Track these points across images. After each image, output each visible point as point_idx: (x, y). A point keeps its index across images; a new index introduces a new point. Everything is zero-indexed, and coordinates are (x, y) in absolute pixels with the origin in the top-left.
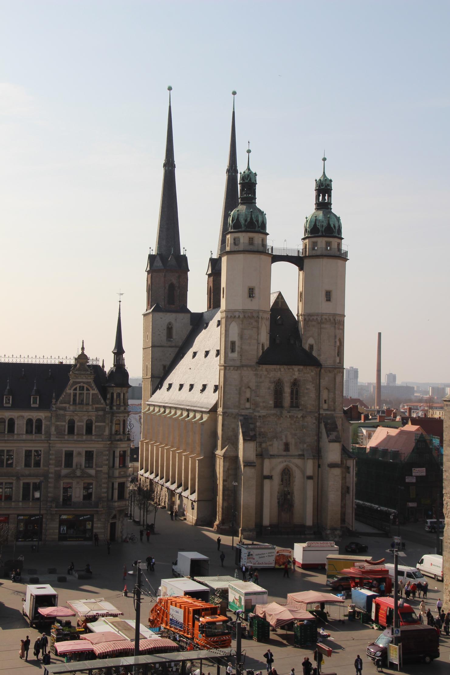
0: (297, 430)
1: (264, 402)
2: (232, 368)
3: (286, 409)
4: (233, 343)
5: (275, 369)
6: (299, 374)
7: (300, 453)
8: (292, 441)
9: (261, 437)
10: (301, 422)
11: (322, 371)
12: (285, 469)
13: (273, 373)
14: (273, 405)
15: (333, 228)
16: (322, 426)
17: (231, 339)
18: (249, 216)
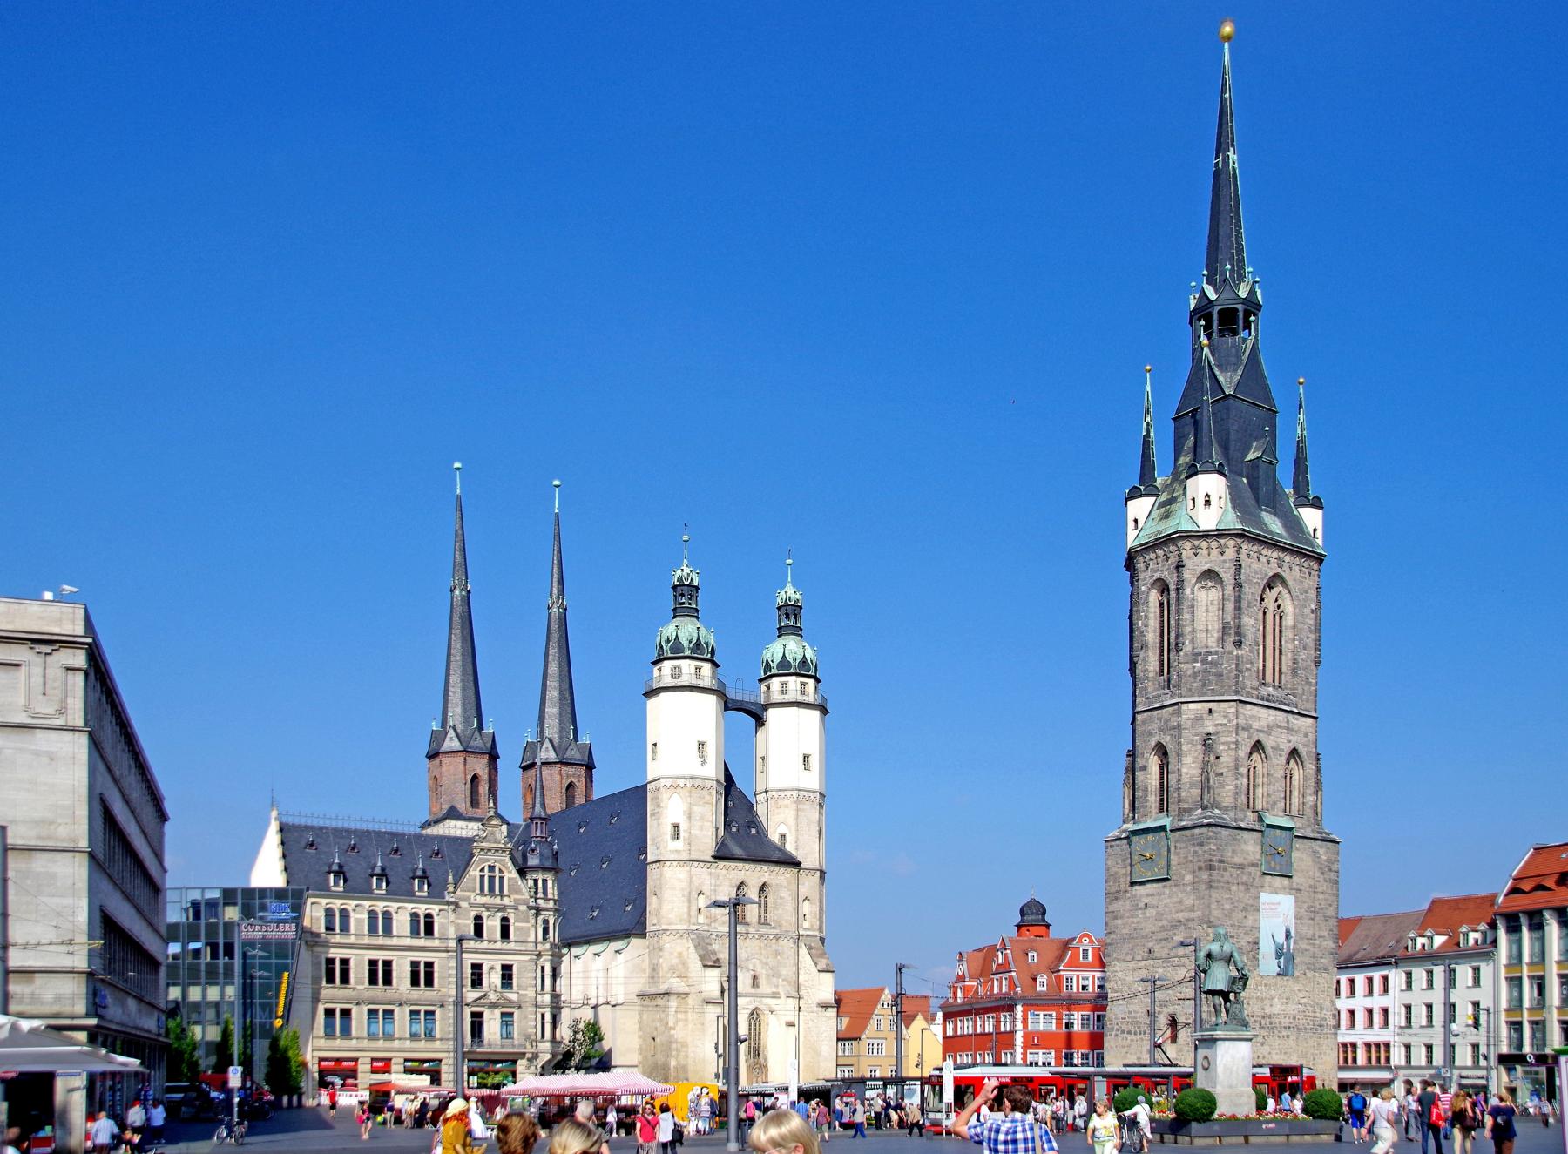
2: (675, 863)
7: (774, 990)
8: (762, 973)
10: (774, 946)
16: (803, 951)
18: (696, 635)
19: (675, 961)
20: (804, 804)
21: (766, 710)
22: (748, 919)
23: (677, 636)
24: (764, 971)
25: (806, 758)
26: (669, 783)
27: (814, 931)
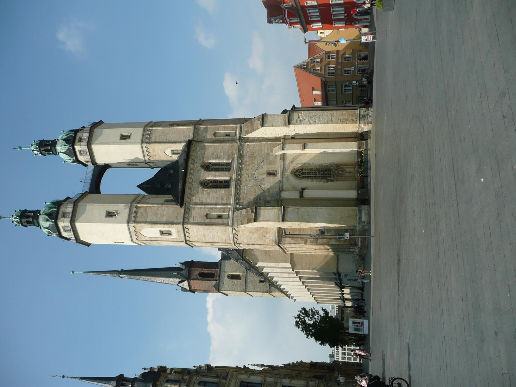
0: (255, 163)
1: (222, 199)
2: (187, 234)
3: (231, 175)
4: (162, 233)
5: (189, 189)
6: (196, 163)
7: (279, 158)
9: (260, 201)
11: (196, 139)
12: (295, 174)
13: (194, 190)
14: (226, 190)
15: (68, 136)
17: (158, 235)
19: (256, 235)
20: (151, 138)
21: (97, 163)
22: (227, 179)
23: (47, 228)
24: (265, 166)
25: (123, 137)
26: (134, 237)
27: (236, 128)
